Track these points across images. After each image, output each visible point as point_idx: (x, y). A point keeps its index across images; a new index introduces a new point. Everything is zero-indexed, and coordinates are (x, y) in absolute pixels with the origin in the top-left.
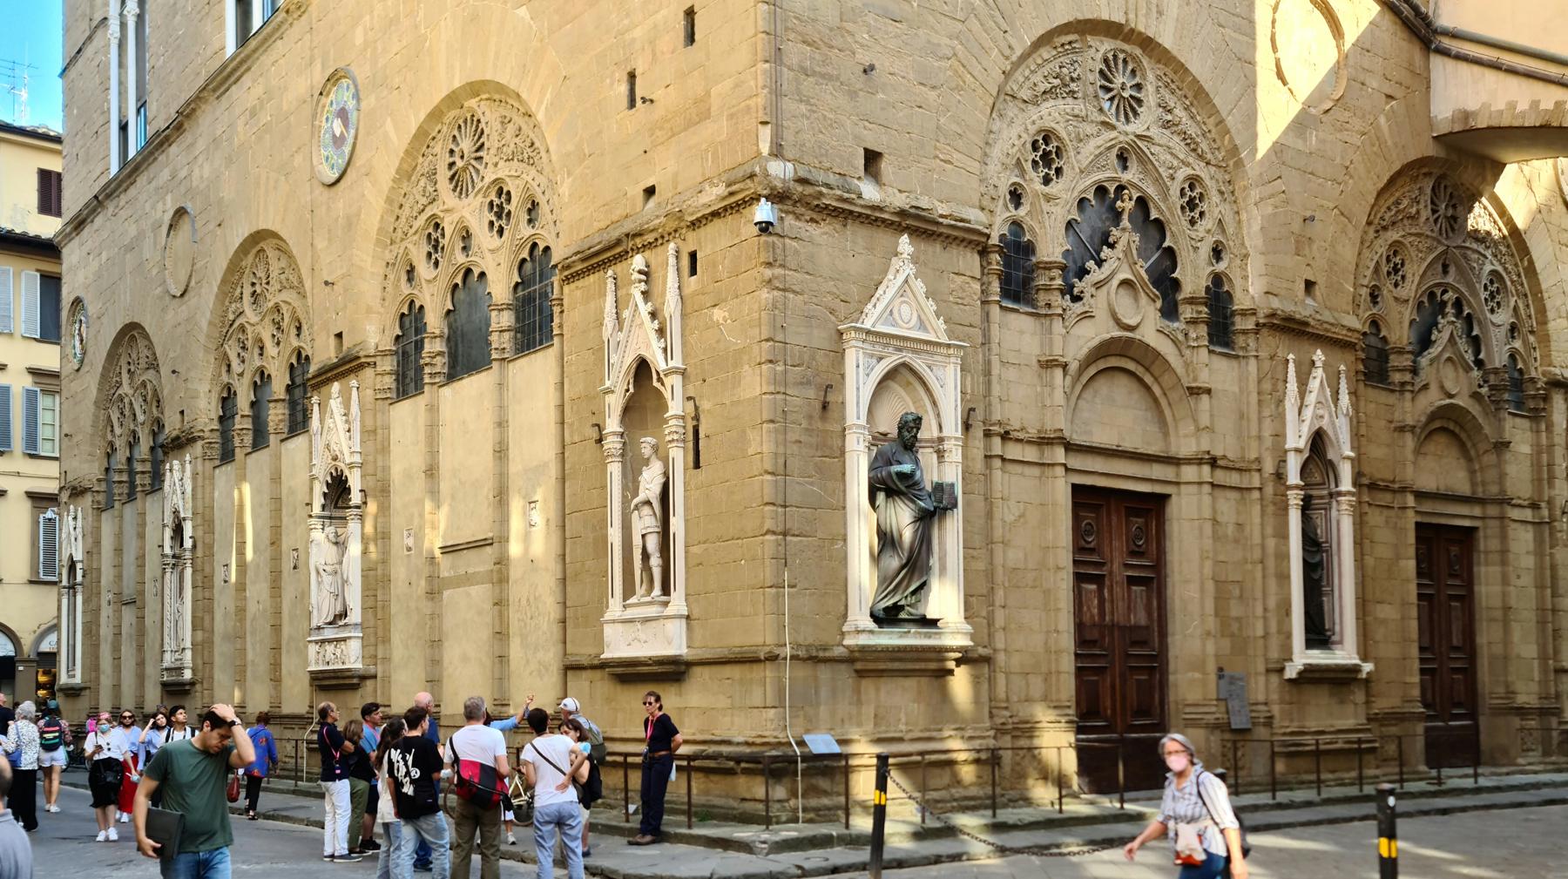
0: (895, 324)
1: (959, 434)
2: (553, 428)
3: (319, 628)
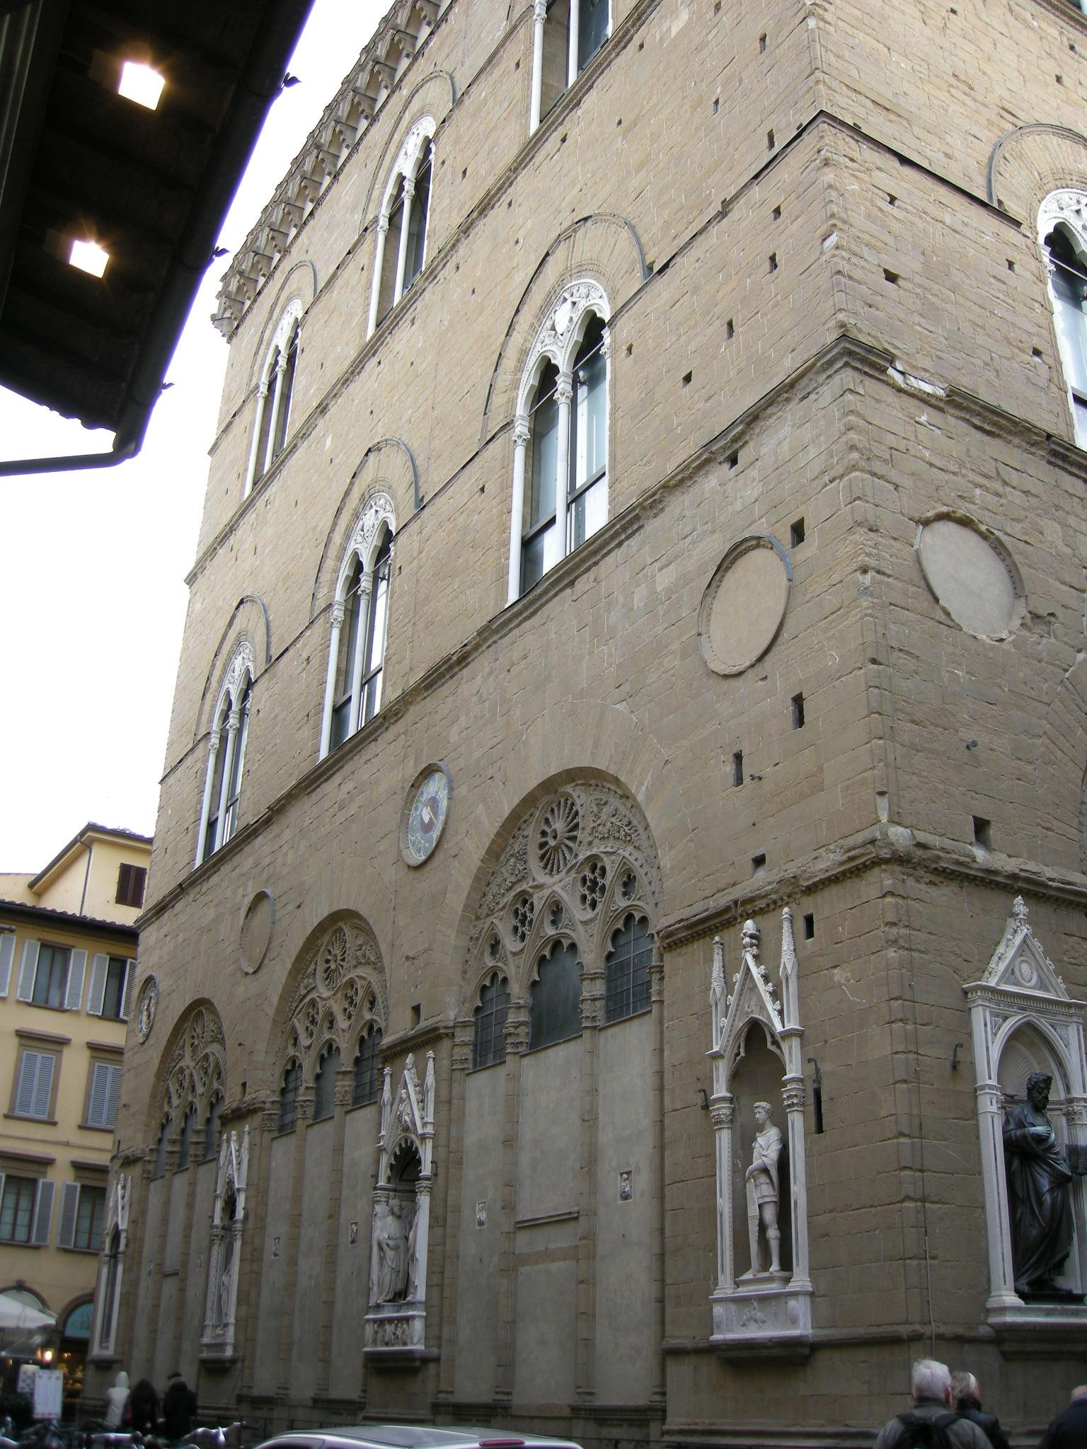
0: (1017, 984)
2: (651, 1096)
3: (378, 1307)
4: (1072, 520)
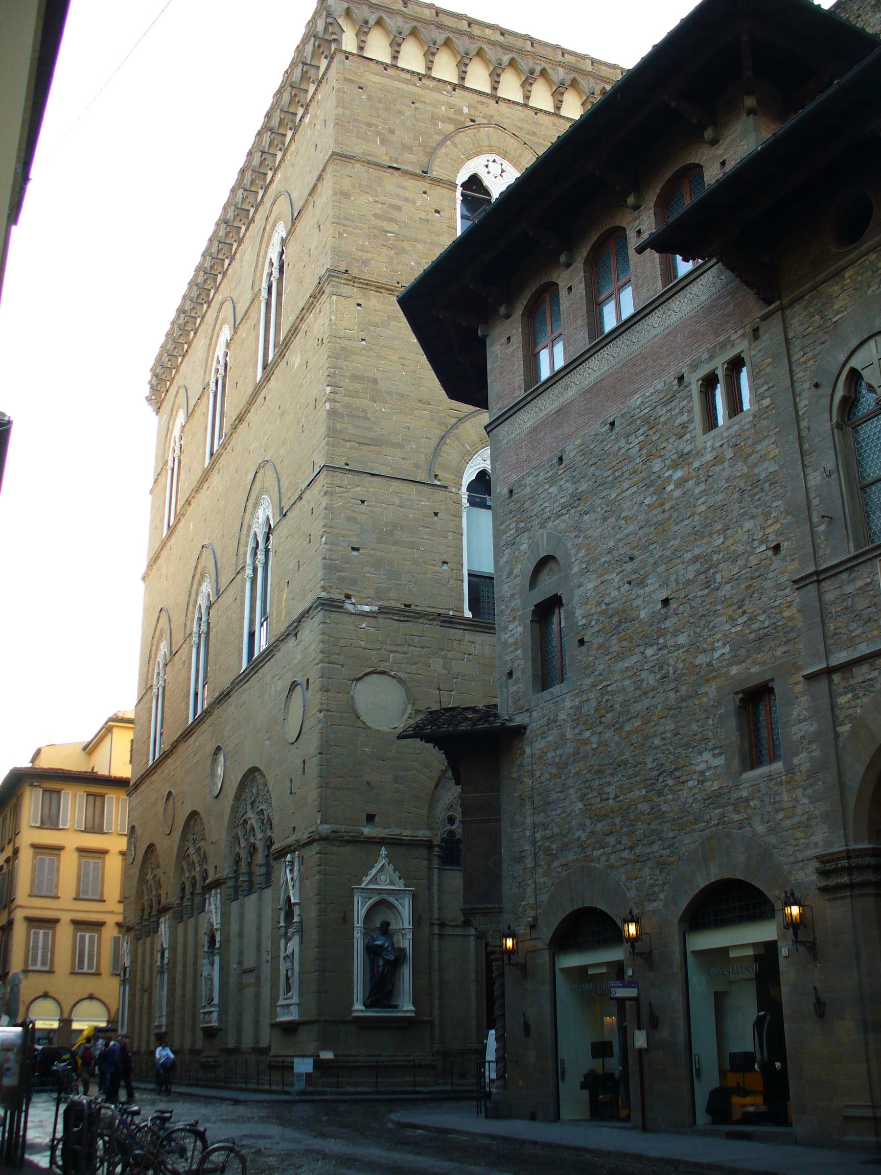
0: (378, 884)
1: (411, 927)
4: (449, 655)
